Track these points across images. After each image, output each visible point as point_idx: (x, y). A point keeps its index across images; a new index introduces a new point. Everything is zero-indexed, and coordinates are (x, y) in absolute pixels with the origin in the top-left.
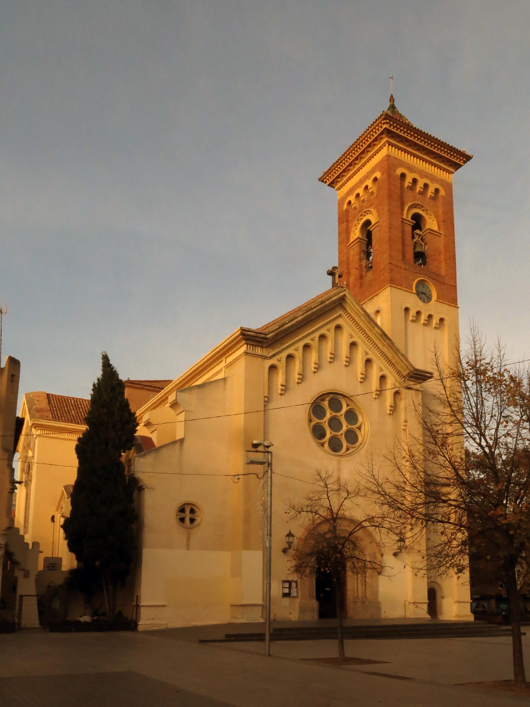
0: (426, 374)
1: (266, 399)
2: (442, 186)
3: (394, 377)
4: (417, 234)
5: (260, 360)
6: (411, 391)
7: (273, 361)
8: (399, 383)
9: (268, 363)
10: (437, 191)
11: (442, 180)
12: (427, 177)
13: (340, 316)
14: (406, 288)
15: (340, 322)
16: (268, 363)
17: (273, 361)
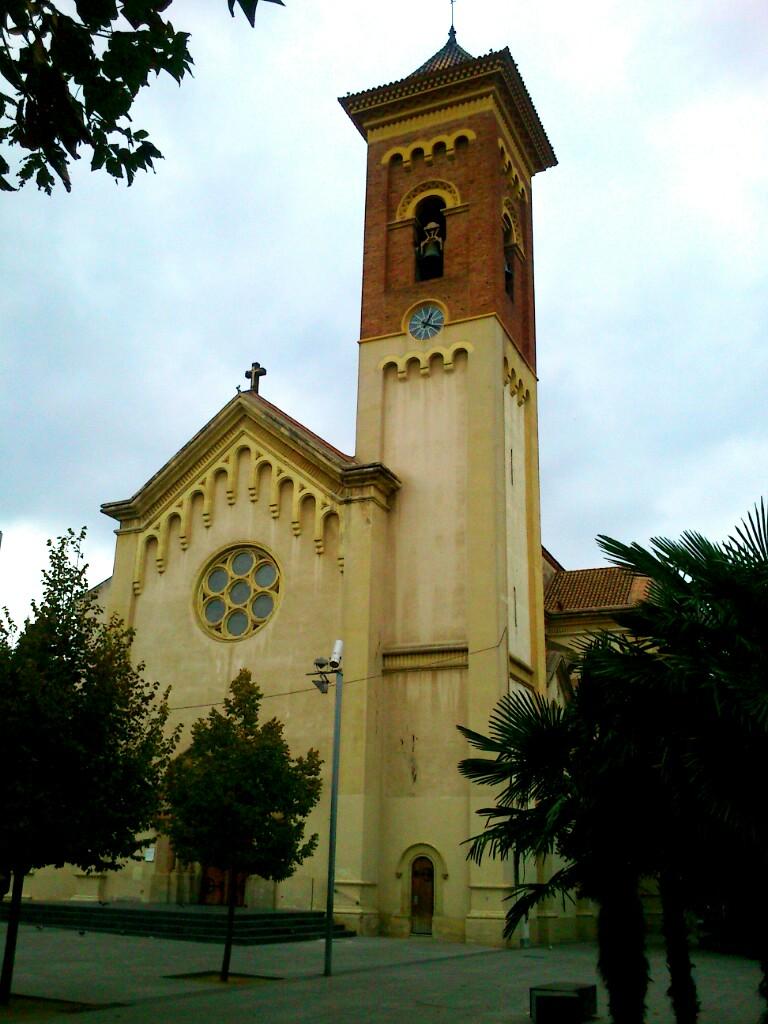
0: (365, 470)
1: (136, 586)
2: (470, 127)
3: (323, 491)
4: (429, 231)
5: (132, 536)
6: (353, 505)
7: (150, 531)
8: (332, 498)
9: (142, 537)
10: (462, 141)
11: (470, 118)
12: (439, 132)
13: (243, 433)
14: (389, 332)
15: (244, 441)
16: (142, 537)
17: (150, 531)
